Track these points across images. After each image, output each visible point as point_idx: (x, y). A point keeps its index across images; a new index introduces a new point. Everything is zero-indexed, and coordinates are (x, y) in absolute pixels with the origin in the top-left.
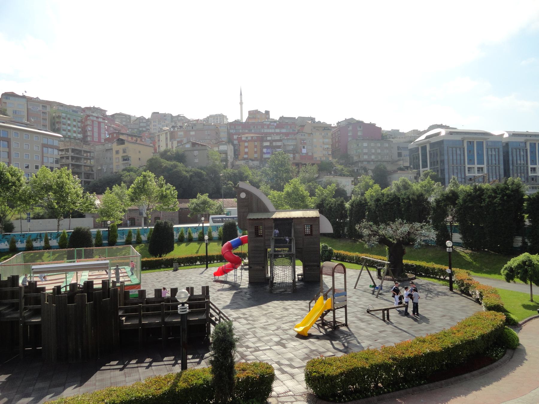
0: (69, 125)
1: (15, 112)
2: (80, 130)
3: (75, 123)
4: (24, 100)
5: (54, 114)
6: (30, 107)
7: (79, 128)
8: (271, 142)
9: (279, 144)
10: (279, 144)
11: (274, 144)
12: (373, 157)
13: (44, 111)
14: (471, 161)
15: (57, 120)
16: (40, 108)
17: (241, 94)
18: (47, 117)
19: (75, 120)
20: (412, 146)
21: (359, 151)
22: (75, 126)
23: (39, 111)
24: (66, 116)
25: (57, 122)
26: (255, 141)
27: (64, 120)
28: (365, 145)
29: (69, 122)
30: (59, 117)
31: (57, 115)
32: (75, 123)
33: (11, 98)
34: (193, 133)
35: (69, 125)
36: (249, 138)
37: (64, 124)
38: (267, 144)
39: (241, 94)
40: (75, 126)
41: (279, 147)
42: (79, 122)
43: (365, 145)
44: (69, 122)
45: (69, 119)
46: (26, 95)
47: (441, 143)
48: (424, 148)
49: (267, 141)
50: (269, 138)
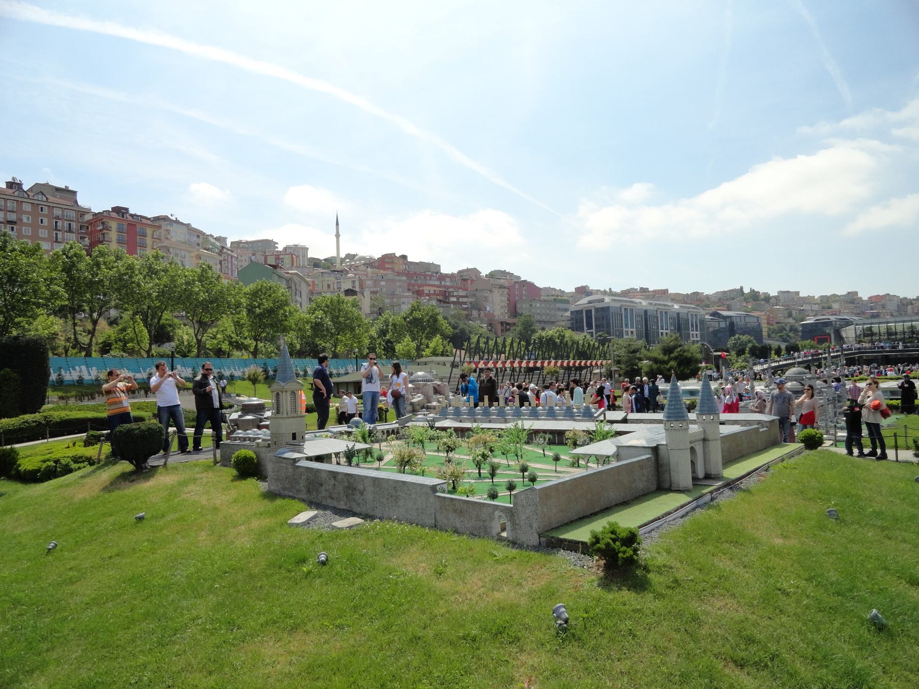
8: (458, 297)
9: (465, 300)
10: (465, 300)
11: (461, 300)
12: (544, 318)
14: (627, 326)
17: (337, 224)
20: (573, 308)
21: (533, 311)
26: (437, 295)
28: (538, 305)
34: (383, 283)
36: (432, 292)
38: (454, 299)
39: (337, 224)
41: (465, 303)
43: (538, 305)
47: (606, 309)
48: (589, 312)
49: (454, 296)
50: (455, 294)
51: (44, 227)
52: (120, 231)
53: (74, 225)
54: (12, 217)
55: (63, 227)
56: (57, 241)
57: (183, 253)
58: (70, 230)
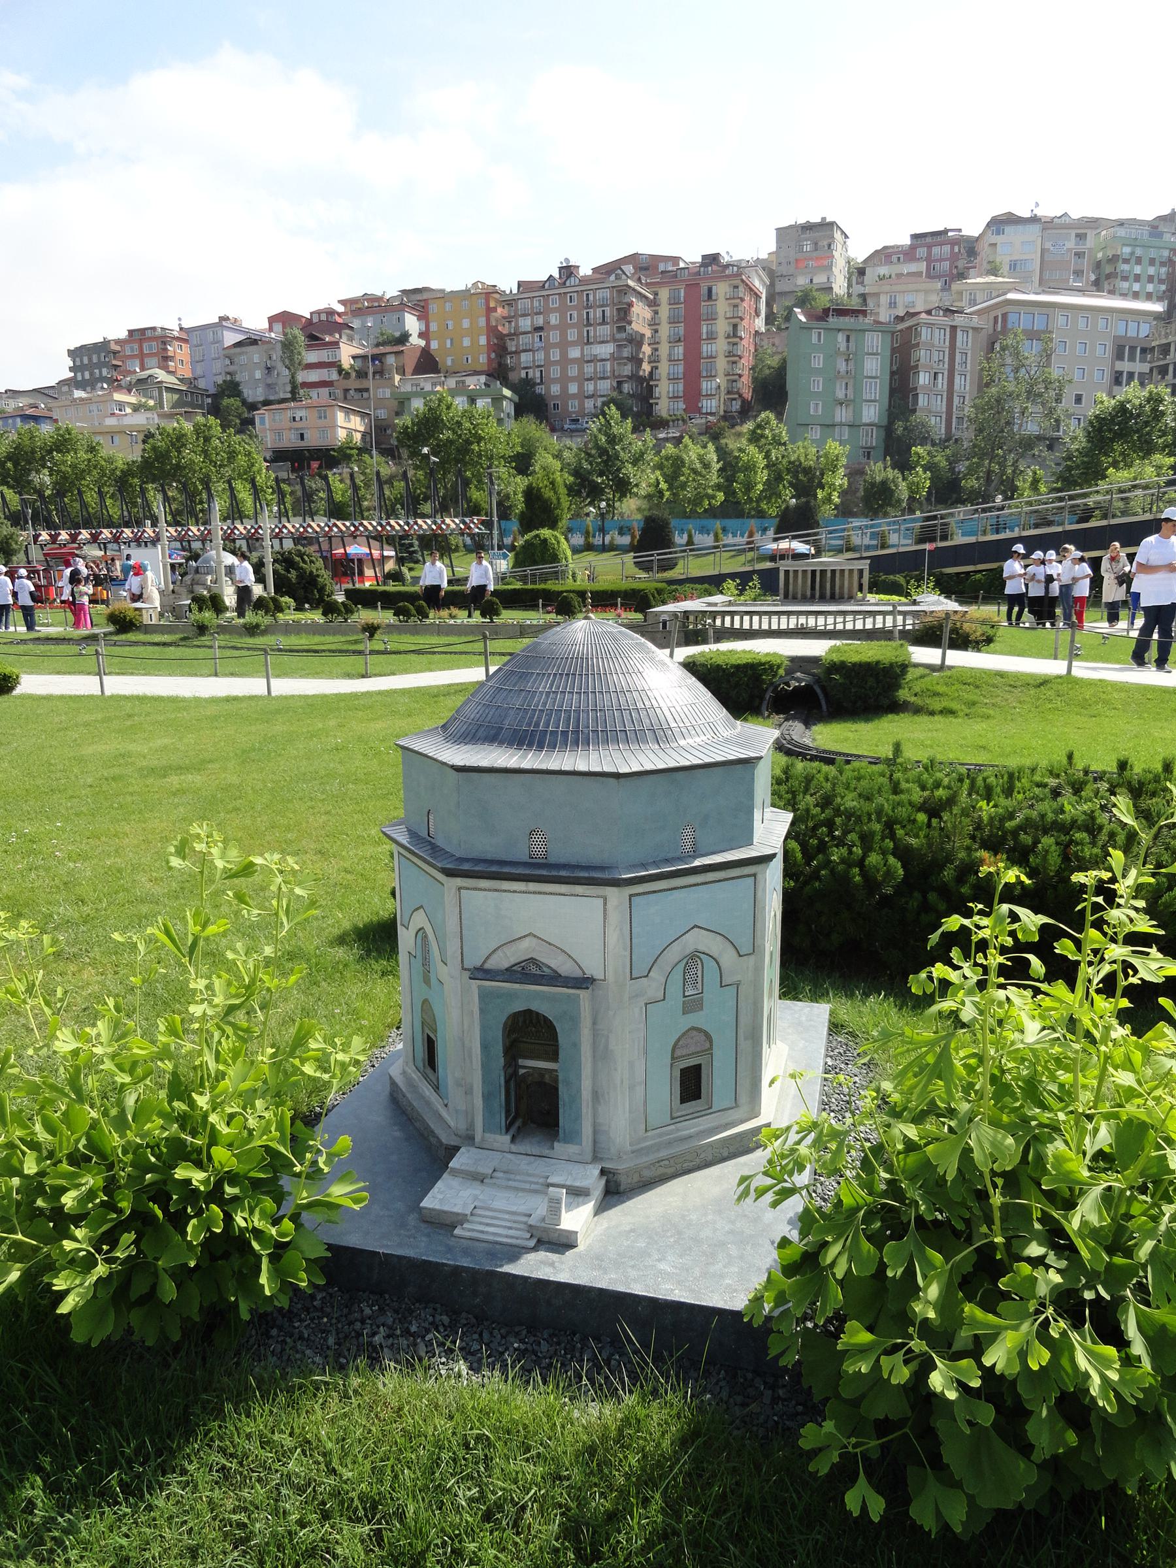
0: (1137, 278)
1: (1013, 266)
2: (1163, 287)
3: (1151, 271)
4: (1036, 229)
5: (1100, 255)
6: (1048, 245)
7: (1161, 282)
13: (1080, 248)
15: (1108, 269)
16: (1071, 243)
18: (1085, 264)
19: (1152, 262)
22: (1151, 279)
23: (1069, 250)
24: (1132, 253)
25: (1109, 276)
27: (1126, 267)
29: (1138, 270)
30: (1114, 259)
31: (1110, 253)
32: (1151, 271)
33: (1008, 229)
35: (1137, 278)
37: (1125, 279)
40: (1151, 279)
42: (1162, 264)
44: (1138, 270)
45: (1139, 261)
46: (1040, 212)
51: (572, 326)
52: (673, 301)
53: (608, 314)
54: (540, 321)
55: (595, 318)
56: (588, 343)
57: (909, 298)
58: (604, 322)
